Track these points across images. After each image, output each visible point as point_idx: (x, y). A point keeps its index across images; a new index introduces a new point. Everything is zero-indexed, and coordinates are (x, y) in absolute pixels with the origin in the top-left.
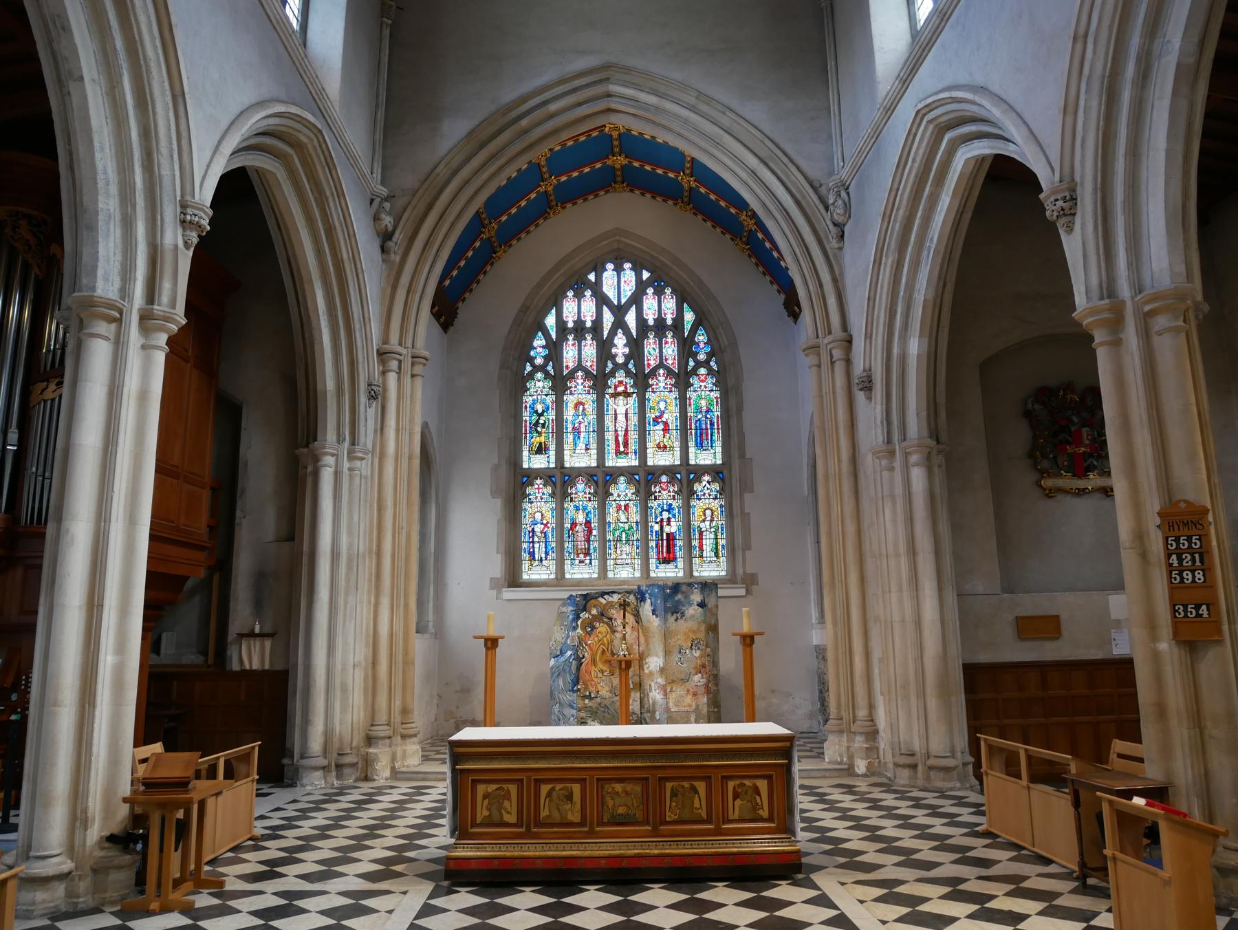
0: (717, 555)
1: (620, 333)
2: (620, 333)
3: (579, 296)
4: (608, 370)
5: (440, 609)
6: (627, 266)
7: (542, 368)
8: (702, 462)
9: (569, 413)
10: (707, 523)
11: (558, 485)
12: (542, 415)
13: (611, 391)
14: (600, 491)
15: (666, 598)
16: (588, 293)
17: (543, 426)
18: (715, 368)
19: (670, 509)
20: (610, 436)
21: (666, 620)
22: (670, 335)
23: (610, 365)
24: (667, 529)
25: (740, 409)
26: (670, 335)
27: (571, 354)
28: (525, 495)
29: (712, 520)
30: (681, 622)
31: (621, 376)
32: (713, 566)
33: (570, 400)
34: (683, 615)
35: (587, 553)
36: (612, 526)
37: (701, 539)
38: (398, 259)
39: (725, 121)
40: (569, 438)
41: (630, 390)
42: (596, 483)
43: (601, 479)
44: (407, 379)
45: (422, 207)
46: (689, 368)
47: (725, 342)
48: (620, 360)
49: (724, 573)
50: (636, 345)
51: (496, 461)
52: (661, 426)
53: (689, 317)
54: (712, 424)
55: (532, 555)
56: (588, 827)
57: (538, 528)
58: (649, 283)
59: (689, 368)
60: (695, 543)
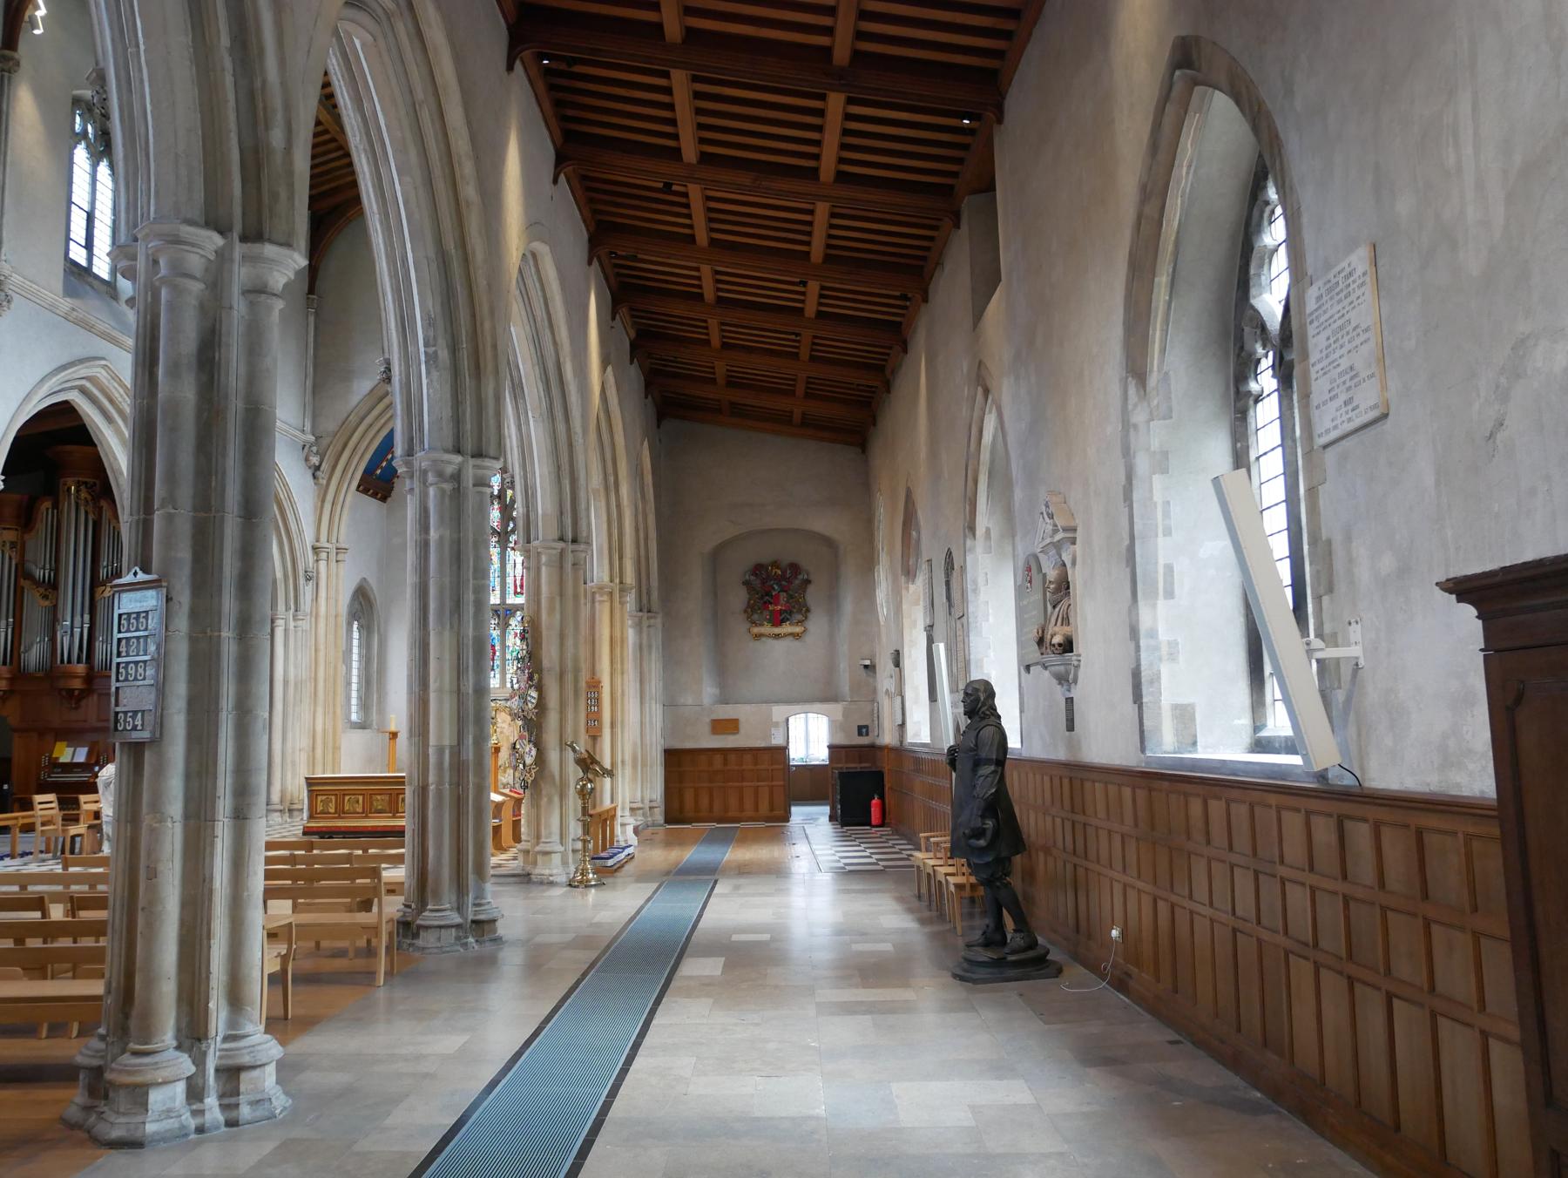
5: (382, 711)
20: (510, 580)
44: (333, 564)
45: (339, 447)
56: (366, 814)
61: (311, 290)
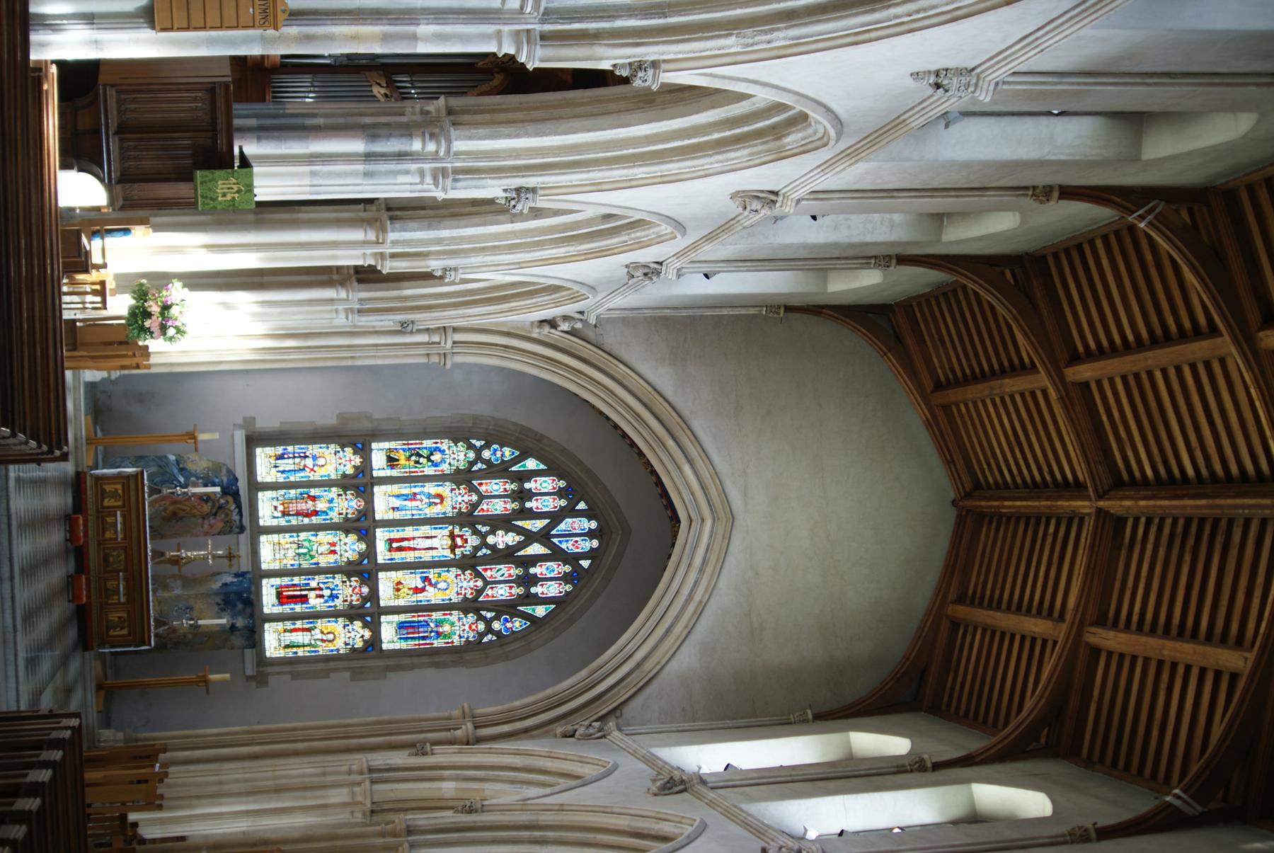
0: (287, 647)
1: (518, 538)
2: (518, 538)
3: (560, 493)
4: (479, 527)
6: (595, 543)
7: (479, 458)
8: (383, 629)
9: (431, 488)
10: (320, 636)
11: (354, 481)
12: (428, 459)
13: (457, 532)
14: (350, 525)
15: (239, 594)
16: (563, 503)
18: (485, 640)
19: (333, 597)
20: (409, 532)
21: (217, 593)
22: (521, 591)
23: (484, 529)
24: (312, 594)
25: (437, 665)
26: (521, 591)
27: (496, 487)
28: (343, 446)
29: (323, 640)
30: (216, 608)
31: (473, 541)
32: (276, 644)
33: (446, 489)
34: (223, 610)
35: (284, 514)
36: (313, 539)
37: (303, 630)
38: (535, 335)
39: (678, 629)
40: (405, 489)
41: (458, 551)
43: (362, 525)
46: (484, 613)
47: (509, 648)
48: (491, 540)
49: (268, 654)
50: (507, 555)
51: (376, 416)
52: (420, 585)
53: (540, 611)
54: (424, 638)
55: (280, 457)
57: (309, 462)
58: (578, 568)
59: (484, 613)
60: (299, 624)
61: (789, 309)
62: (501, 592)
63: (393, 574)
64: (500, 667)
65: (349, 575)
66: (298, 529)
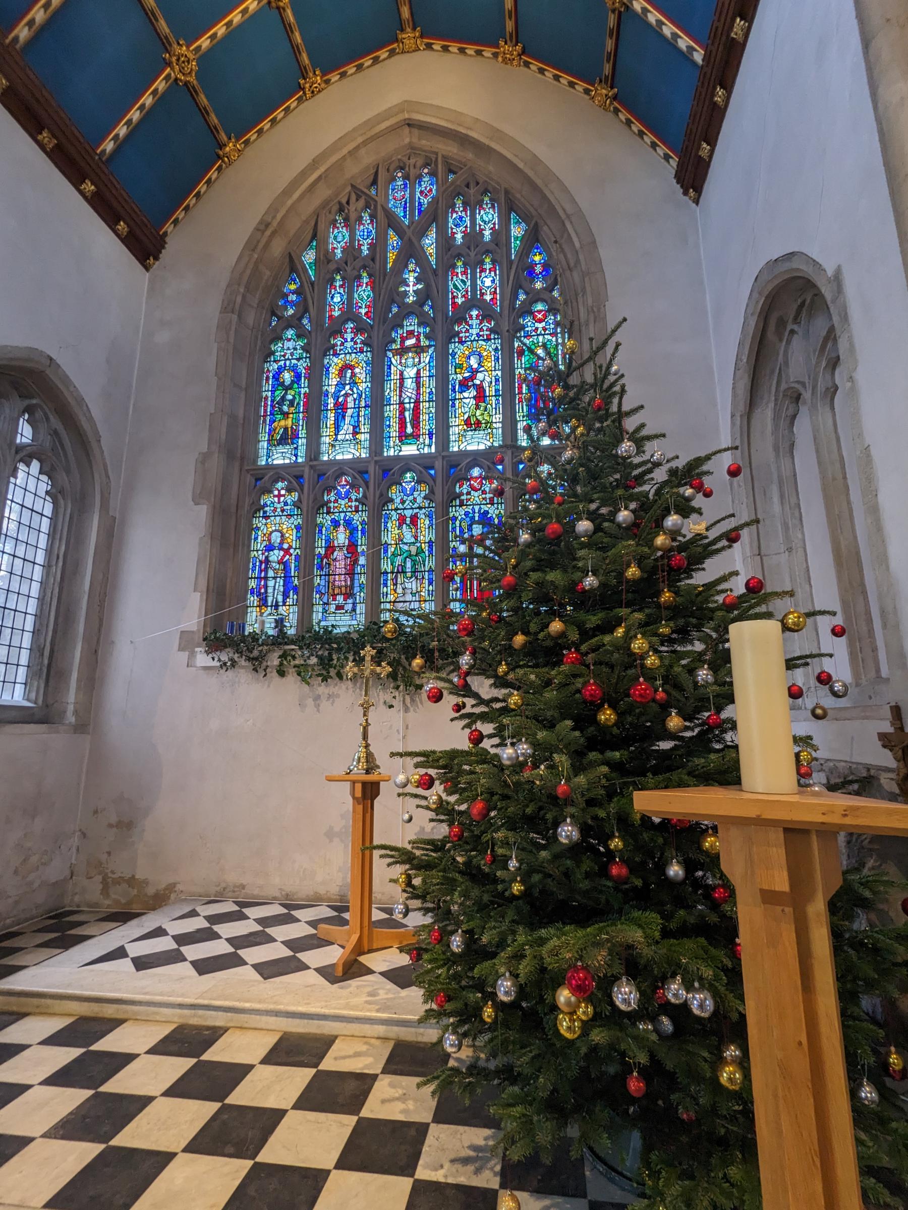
12: (290, 387)
17: (291, 403)
20: (392, 411)
27: (337, 299)
28: (257, 509)
31: (412, 324)
33: (335, 363)
35: (349, 595)
36: (391, 549)
41: (424, 342)
42: (367, 483)
43: (377, 477)
52: (473, 393)
62: (488, 282)
63: (454, 431)
64: (606, 253)
65: (452, 497)
66: (376, 576)
